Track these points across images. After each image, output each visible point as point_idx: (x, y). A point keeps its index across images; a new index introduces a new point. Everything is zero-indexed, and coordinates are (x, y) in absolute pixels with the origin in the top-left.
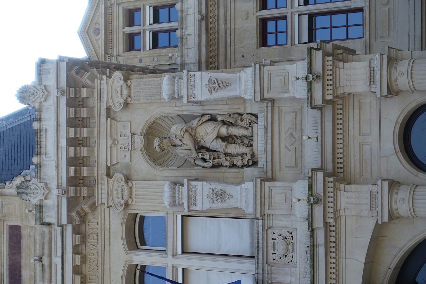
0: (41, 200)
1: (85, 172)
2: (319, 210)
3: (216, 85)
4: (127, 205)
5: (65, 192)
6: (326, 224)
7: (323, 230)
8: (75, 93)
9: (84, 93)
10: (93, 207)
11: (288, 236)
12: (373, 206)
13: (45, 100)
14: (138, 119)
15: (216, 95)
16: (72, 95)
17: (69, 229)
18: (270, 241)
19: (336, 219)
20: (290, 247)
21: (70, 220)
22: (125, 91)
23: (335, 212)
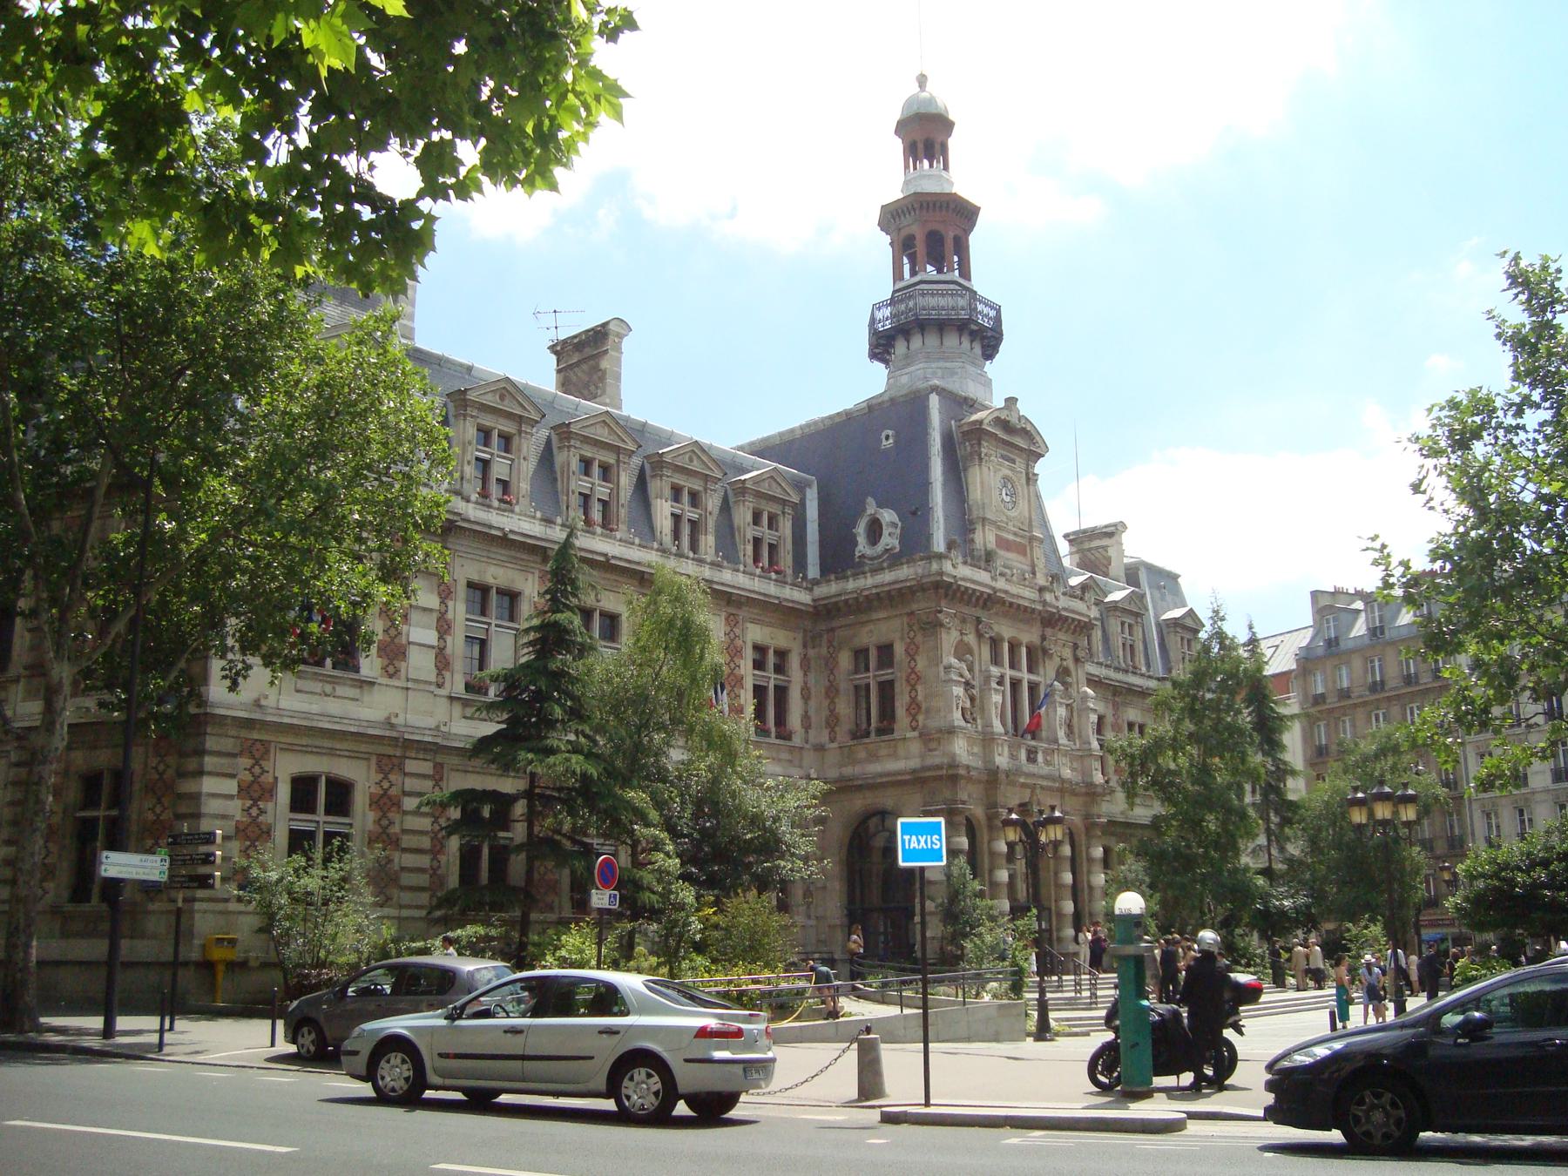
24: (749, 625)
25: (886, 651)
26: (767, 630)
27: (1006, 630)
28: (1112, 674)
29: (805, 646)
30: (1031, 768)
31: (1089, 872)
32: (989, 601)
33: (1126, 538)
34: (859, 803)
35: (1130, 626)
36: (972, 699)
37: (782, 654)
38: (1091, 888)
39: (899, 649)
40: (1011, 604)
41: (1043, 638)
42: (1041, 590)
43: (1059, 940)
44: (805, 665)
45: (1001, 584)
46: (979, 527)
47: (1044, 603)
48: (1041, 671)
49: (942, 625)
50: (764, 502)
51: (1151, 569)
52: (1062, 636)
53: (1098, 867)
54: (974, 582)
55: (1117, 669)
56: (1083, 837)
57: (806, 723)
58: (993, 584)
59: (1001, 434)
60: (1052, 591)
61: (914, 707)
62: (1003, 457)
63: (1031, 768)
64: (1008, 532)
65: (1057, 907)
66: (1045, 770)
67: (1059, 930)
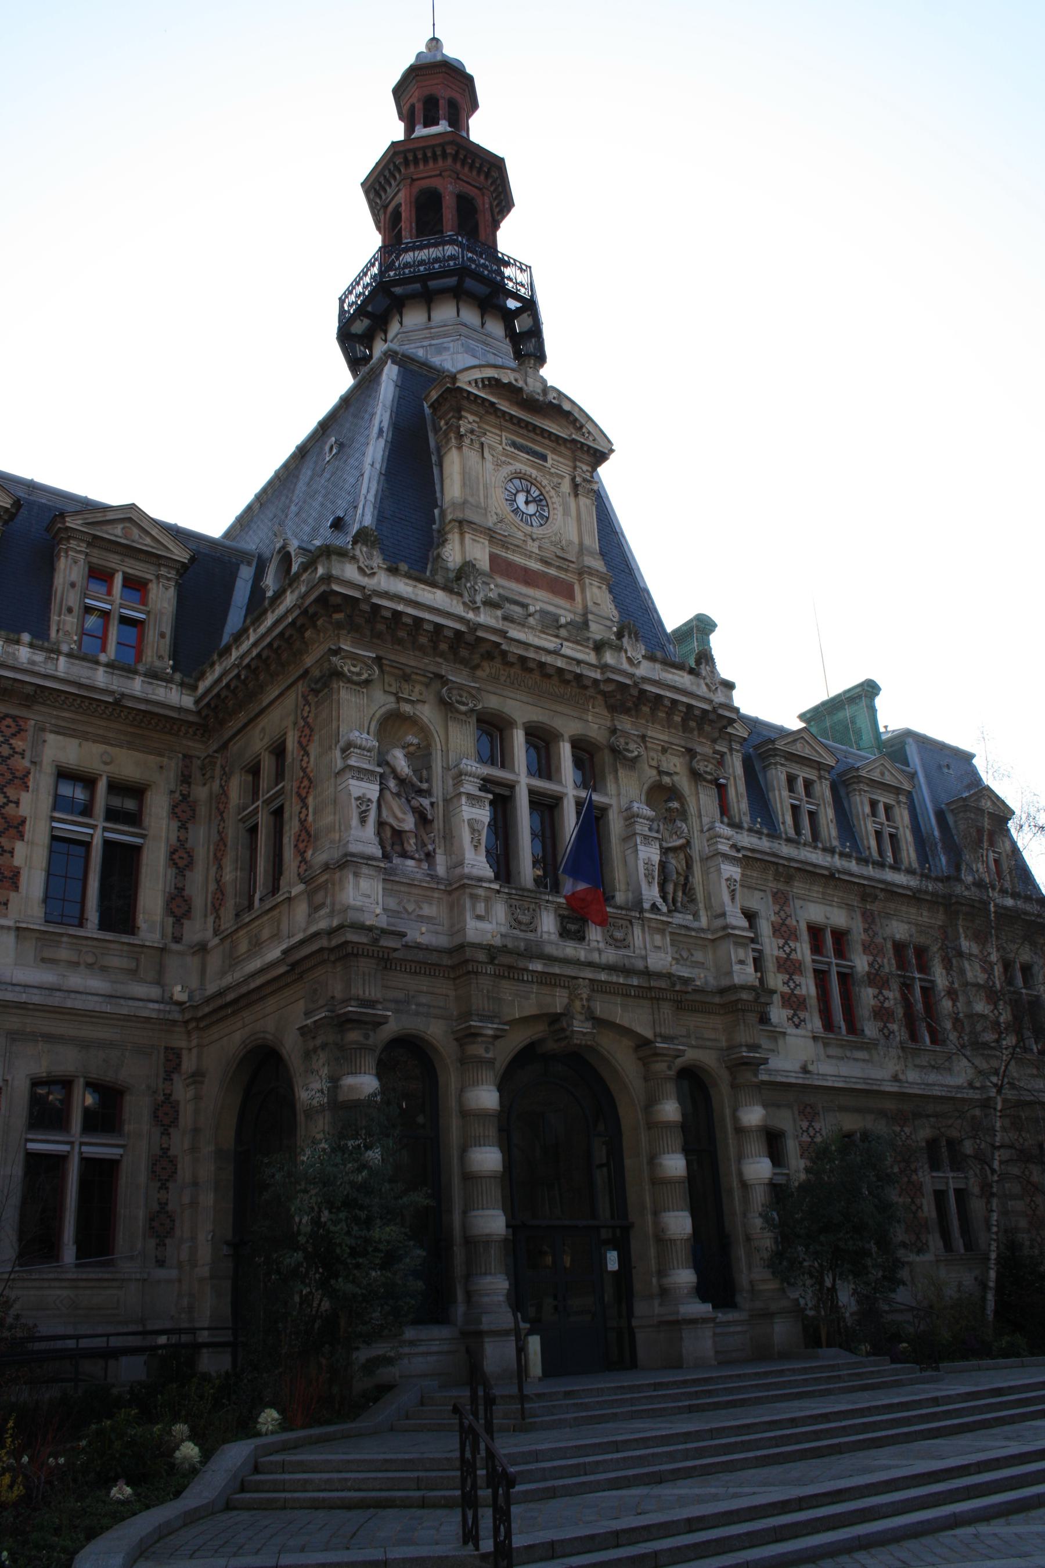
0: (626, 651)
1: (646, 709)
2: (663, 984)
3: (732, 888)
4: (615, 751)
5: (636, 684)
6: (650, 988)
7: (647, 985)
8: (712, 721)
9: (707, 728)
10: (612, 709)
11: (626, 943)
12: (666, 1038)
13: (707, 685)
14: (684, 783)
15: (724, 884)
16: (712, 716)
17: (597, 675)
18: (621, 922)
19: (652, 999)
20: (618, 944)
21: (609, 680)
22: (709, 777)
23: (658, 999)
24: (50, 737)
25: (279, 751)
26: (97, 749)
27: (521, 709)
28: (853, 866)
29: (186, 779)
30: (570, 949)
31: (740, 1158)
32: (466, 646)
33: (880, 702)
34: (232, 1038)
35: (888, 808)
36: (423, 819)
37: (137, 791)
38: (745, 1185)
39: (291, 744)
40: (523, 659)
41: (613, 731)
42: (599, 647)
43: (664, 1292)
44: (183, 811)
45: (485, 618)
46: (454, 537)
47: (604, 667)
48: (611, 787)
49: (338, 674)
50: (115, 558)
51: (924, 742)
52: (658, 734)
53: (756, 1146)
54: (416, 604)
55: (863, 861)
56: (725, 1088)
57: (178, 906)
58: (470, 615)
59: (504, 406)
60: (620, 649)
61: (307, 836)
62: (514, 444)
63: (570, 949)
64: (529, 555)
65: (656, 1223)
66: (610, 956)
67: (662, 1273)
